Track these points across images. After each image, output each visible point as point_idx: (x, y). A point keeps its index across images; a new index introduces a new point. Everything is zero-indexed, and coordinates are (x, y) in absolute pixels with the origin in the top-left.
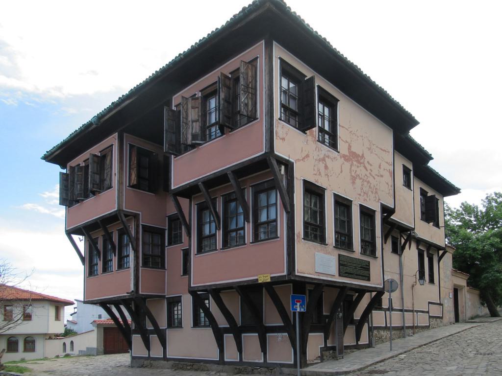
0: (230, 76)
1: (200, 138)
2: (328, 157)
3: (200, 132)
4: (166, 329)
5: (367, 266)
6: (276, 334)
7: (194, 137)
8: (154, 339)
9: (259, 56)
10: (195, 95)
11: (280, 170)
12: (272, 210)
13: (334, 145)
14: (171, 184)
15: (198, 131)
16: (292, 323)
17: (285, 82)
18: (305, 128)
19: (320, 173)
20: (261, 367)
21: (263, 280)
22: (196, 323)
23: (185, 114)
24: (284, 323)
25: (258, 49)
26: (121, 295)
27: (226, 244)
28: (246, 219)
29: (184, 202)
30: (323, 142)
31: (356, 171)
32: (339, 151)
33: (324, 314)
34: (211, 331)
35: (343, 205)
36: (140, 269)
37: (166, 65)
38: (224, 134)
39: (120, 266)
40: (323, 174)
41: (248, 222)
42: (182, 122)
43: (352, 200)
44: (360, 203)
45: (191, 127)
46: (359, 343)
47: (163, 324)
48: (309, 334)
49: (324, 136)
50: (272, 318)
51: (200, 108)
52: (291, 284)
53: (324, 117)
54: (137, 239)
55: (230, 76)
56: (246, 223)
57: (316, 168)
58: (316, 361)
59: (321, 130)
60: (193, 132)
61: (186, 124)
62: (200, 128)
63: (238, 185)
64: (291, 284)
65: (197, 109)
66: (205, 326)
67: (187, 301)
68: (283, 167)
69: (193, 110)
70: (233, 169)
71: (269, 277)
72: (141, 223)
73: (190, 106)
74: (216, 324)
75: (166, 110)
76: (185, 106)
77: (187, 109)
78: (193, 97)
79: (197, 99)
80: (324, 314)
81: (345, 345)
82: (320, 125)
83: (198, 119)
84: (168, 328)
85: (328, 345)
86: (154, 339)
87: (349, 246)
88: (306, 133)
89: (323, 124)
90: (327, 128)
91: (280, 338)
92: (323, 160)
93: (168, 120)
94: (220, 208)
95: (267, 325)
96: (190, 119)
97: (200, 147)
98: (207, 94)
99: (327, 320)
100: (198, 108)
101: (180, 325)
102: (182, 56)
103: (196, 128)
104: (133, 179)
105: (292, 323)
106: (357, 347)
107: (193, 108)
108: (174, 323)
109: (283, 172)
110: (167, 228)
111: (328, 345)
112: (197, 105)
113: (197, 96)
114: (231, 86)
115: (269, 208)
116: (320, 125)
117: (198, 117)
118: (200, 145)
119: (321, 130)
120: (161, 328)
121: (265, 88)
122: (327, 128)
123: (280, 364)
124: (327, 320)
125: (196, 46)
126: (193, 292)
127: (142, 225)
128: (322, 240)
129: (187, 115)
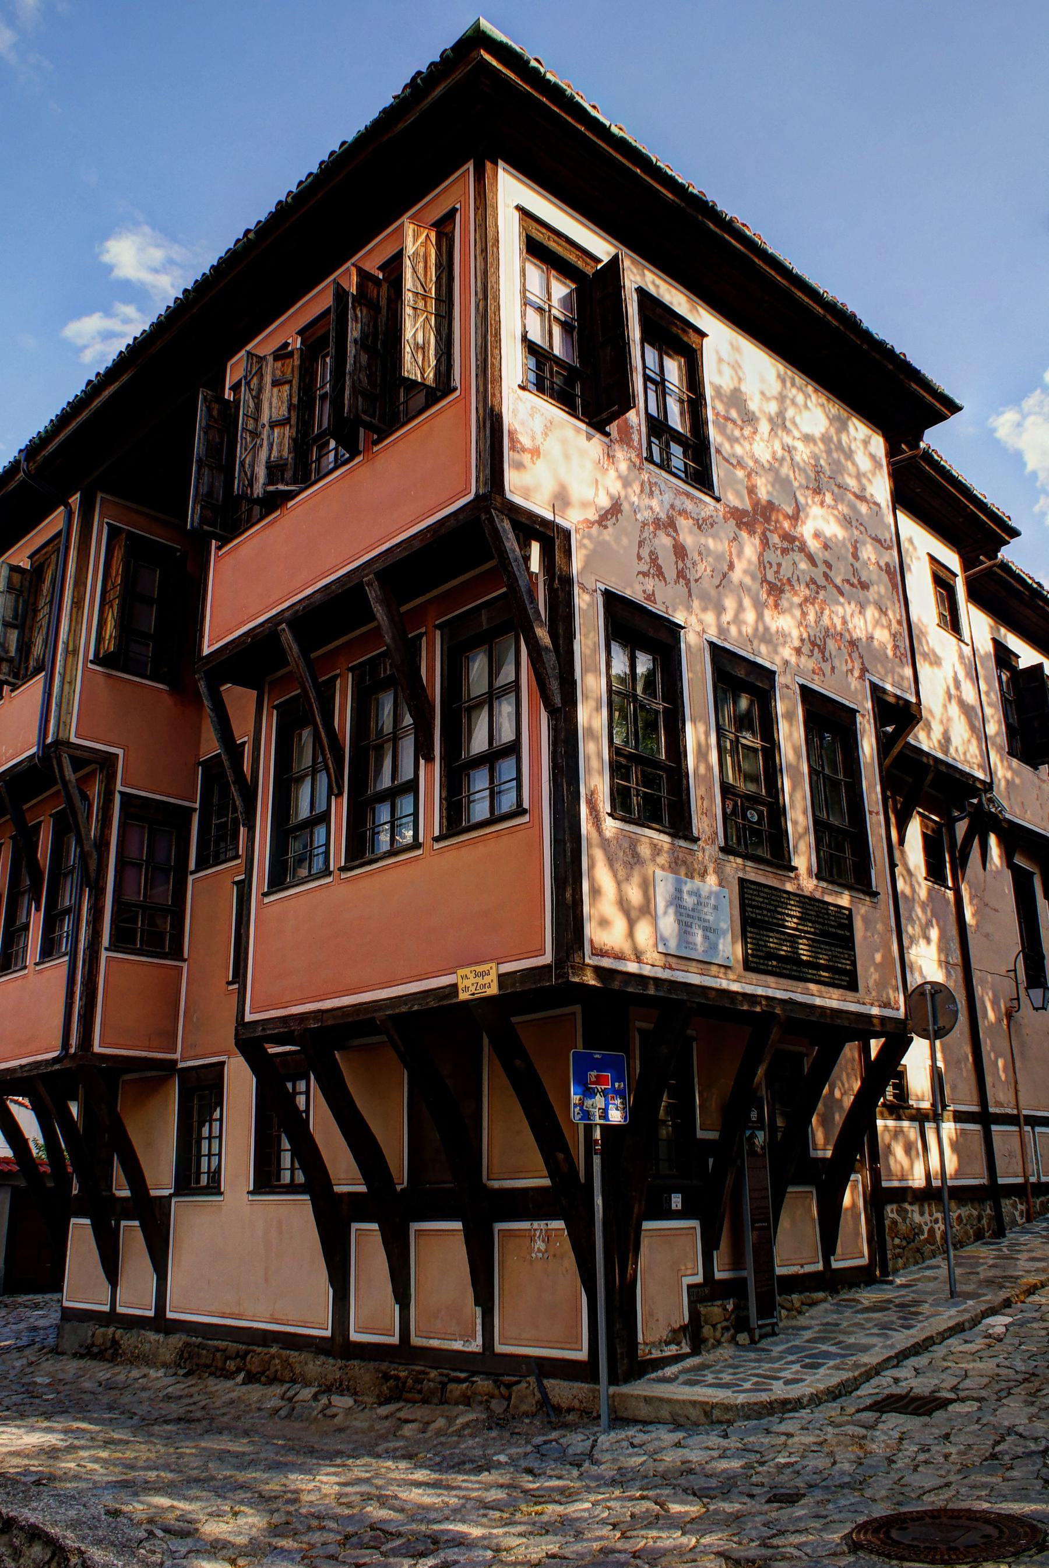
0: (381, 276)
1: (289, 475)
2: (683, 512)
3: (291, 456)
4: (171, 1196)
5: (841, 926)
6: (525, 1225)
7: (274, 471)
8: (131, 1233)
9: (458, 206)
10: (286, 344)
11: (527, 559)
12: (506, 709)
13: (700, 476)
14: (202, 636)
15: (285, 454)
16: (583, 1180)
17: (535, 274)
18: (604, 416)
19: (659, 568)
20: (474, 1373)
21: (472, 989)
22: (266, 1180)
23: (252, 404)
24: (551, 1176)
26: (39, 1058)
27: (360, 849)
28: (423, 750)
29: (240, 701)
30: (665, 466)
31: (779, 565)
32: (717, 494)
33: (700, 1134)
34: (309, 1208)
35: (741, 680)
36: (104, 954)
37: (213, 267)
38: (359, 453)
39: (48, 951)
40: (670, 573)
41: (429, 759)
42: (243, 428)
43: (774, 668)
44: (802, 681)
45: (265, 443)
46: (835, 1265)
47: (161, 1179)
48: (647, 1225)
49: (668, 446)
50: (513, 1161)
51: (295, 383)
52: (577, 1009)
53: (664, 386)
54: (102, 844)
55: (381, 276)
56: (422, 762)
57: (645, 553)
58: (672, 1350)
59: (657, 427)
61: (255, 434)
63: (401, 624)
64: (577, 1009)
65: (287, 387)
66: (292, 1189)
67: (240, 1084)
68: (535, 548)
70: (378, 566)
71: (493, 976)
72: (119, 787)
73: (268, 380)
74: (328, 1183)
75: (205, 399)
76: (255, 381)
77: (260, 390)
78: (282, 354)
79: (291, 355)
80: (700, 1134)
81: (779, 1271)
82: (653, 410)
84: (176, 1194)
85: (719, 1275)
86: (131, 1233)
87: (779, 858)
89: (663, 407)
90: (676, 420)
91: (540, 1245)
92: (669, 525)
93: (207, 430)
94: (344, 719)
95: (496, 1184)
96: (265, 419)
97: (290, 504)
99: (711, 1161)
100: (290, 382)
101: (214, 1188)
102: (251, 236)
103: (281, 444)
104: (107, 637)
105: (583, 1180)
106: (831, 1282)
107: (276, 383)
108: (195, 1178)
109: (535, 565)
110: (197, 806)
111: (719, 1275)
112: (289, 376)
113: (290, 348)
114: (383, 303)
115: (496, 704)
116: (653, 410)
117: (289, 413)
118: (290, 496)
119: (657, 427)
120: (153, 1193)
121: (476, 294)
122: (676, 420)
123: (540, 1361)
124: (711, 1161)
125: (289, 200)
126: (250, 1042)
127: (120, 792)
128: (679, 825)
129: (258, 407)
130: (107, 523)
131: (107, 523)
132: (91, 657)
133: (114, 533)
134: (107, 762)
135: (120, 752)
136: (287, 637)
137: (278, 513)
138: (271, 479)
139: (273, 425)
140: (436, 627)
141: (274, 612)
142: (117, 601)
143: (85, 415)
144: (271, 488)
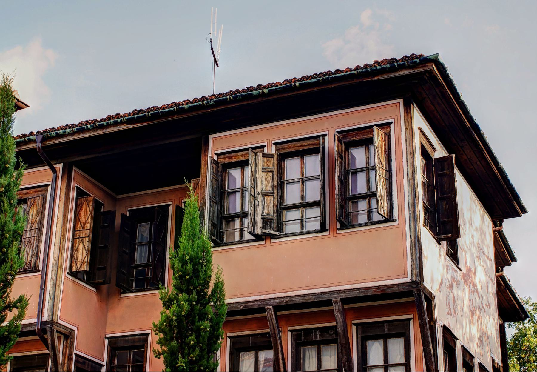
1: (274, 225)
3: (275, 215)
15: (271, 213)
25: (391, 110)
60: (265, 211)
62: (275, 209)
65: (270, 174)
69: (264, 174)
73: (259, 167)
83: (273, 193)
88: (440, 244)
96: (259, 190)
97: (273, 241)
98: (287, 152)
100: (273, 172)
112: (271, 168)
130: (77, 187)
131: (77, 187)
132: (68, 270)
133: (81, 194)
134: (68, 336)
135: (75, 328)
136: (270, 313)
137: (263, 242)
138: (264, 227)
139: (264, 194)
140: (355, 324)
141: (262, 297)
142: (87, 239)
143: (99, 132)
144: (266, 231)
